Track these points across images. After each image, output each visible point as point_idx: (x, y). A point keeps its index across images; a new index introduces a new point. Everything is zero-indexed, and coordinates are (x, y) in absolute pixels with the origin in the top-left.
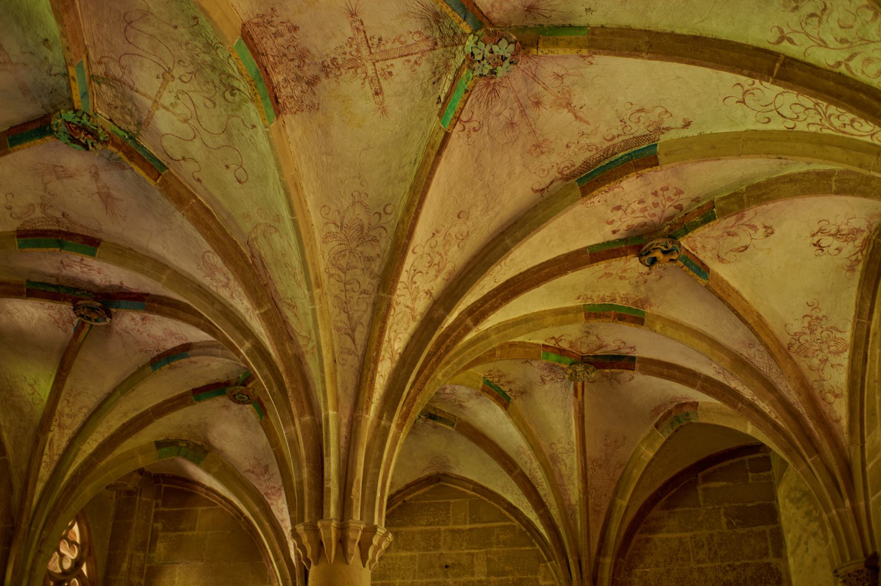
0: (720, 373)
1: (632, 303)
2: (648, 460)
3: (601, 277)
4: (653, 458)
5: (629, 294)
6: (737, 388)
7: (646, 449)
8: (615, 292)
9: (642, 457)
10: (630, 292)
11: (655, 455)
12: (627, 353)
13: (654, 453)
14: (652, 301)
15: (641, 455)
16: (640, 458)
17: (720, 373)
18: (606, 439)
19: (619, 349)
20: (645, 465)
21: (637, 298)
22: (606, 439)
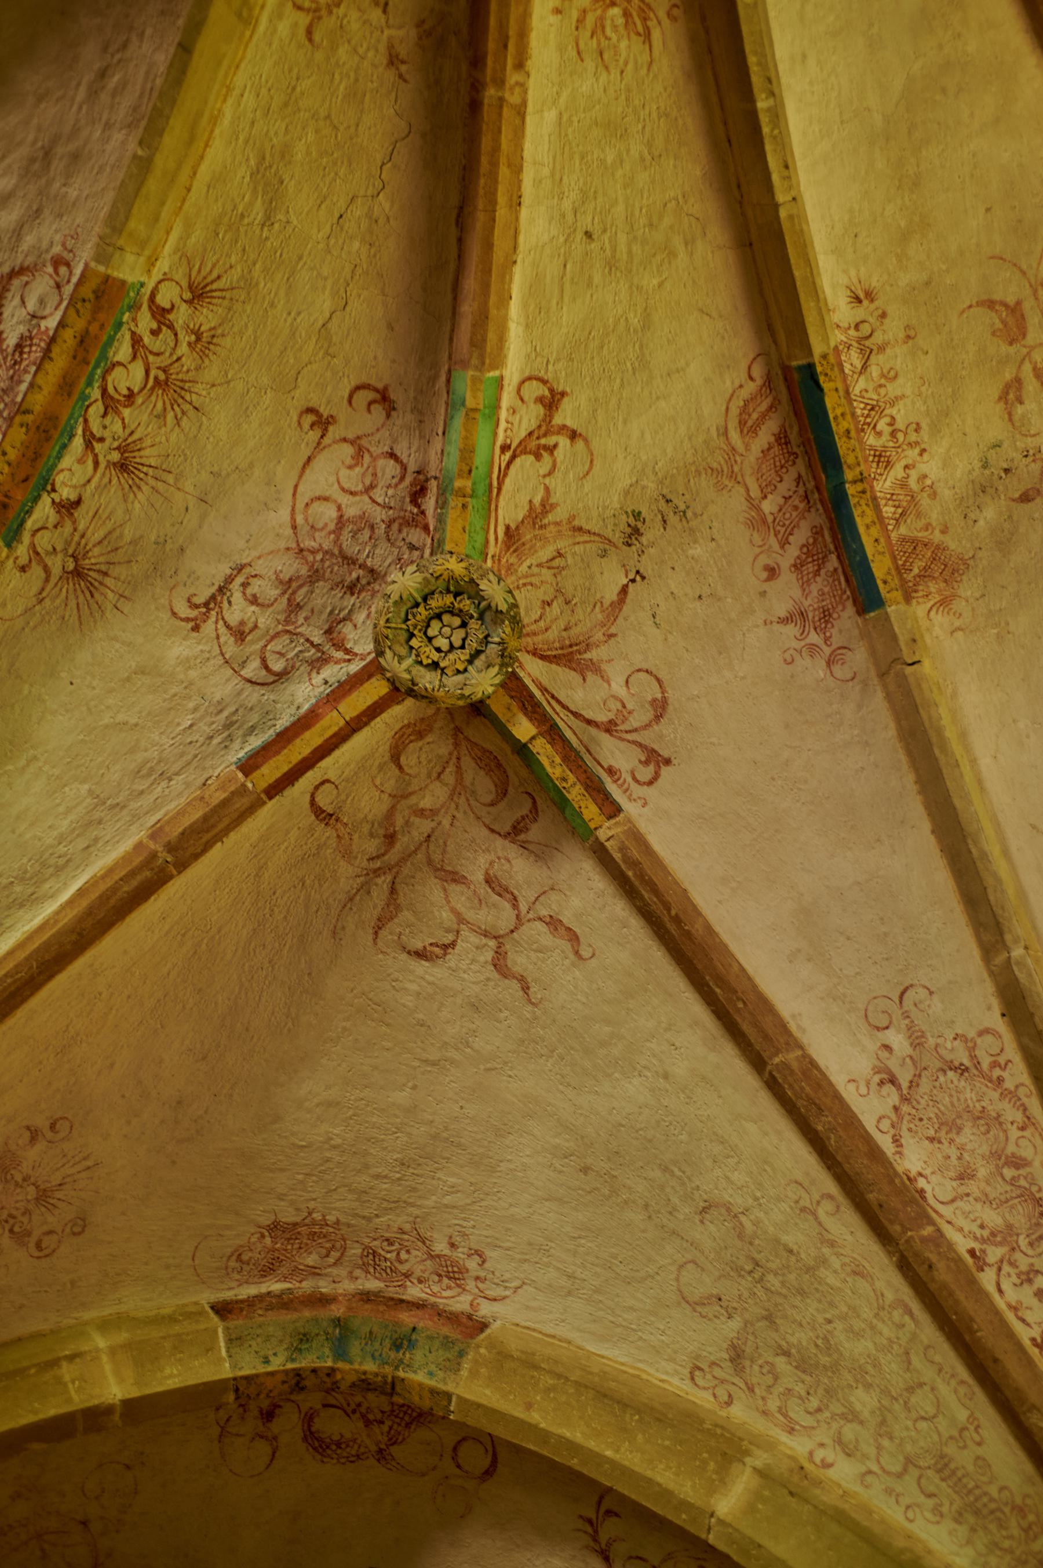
0: (893, 1081)
1: (903, 540)
2: (78, 1400)
3: (990, 304)
4: (107, 1411)
5: (934, 495)
6: (921, 1183)
7: (113, 1351)
8: (925, 434)
9: (66, 1371)
10: (946, 494)
11: (130, 1406)
12: (611, 771)
13: (135, 1393)
14: (968, 589)
15: (71, 1358)
16: (55, 1363)
17: (893, 1081)
18: (34, 1135)
19: (610, 727)
20: (52, 1410)
21: (937, 537)
22: (34, 1135)
